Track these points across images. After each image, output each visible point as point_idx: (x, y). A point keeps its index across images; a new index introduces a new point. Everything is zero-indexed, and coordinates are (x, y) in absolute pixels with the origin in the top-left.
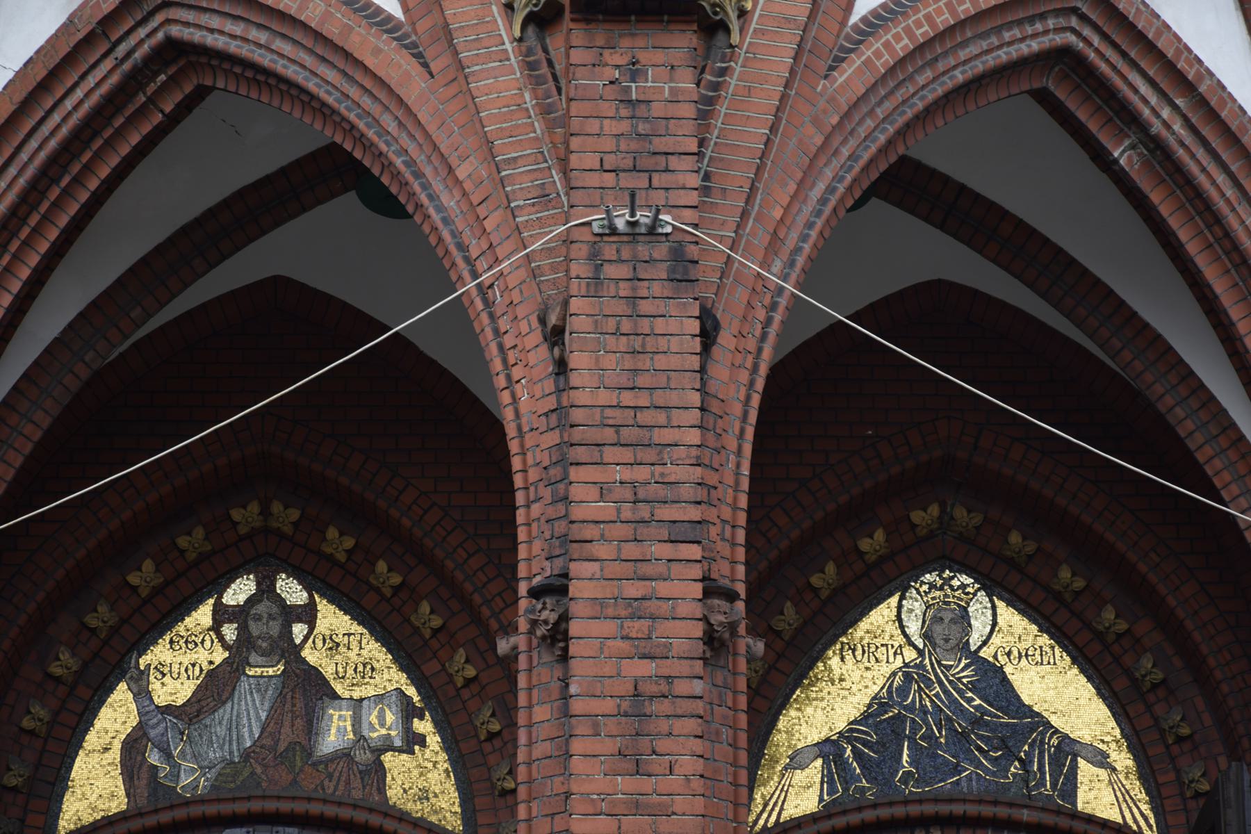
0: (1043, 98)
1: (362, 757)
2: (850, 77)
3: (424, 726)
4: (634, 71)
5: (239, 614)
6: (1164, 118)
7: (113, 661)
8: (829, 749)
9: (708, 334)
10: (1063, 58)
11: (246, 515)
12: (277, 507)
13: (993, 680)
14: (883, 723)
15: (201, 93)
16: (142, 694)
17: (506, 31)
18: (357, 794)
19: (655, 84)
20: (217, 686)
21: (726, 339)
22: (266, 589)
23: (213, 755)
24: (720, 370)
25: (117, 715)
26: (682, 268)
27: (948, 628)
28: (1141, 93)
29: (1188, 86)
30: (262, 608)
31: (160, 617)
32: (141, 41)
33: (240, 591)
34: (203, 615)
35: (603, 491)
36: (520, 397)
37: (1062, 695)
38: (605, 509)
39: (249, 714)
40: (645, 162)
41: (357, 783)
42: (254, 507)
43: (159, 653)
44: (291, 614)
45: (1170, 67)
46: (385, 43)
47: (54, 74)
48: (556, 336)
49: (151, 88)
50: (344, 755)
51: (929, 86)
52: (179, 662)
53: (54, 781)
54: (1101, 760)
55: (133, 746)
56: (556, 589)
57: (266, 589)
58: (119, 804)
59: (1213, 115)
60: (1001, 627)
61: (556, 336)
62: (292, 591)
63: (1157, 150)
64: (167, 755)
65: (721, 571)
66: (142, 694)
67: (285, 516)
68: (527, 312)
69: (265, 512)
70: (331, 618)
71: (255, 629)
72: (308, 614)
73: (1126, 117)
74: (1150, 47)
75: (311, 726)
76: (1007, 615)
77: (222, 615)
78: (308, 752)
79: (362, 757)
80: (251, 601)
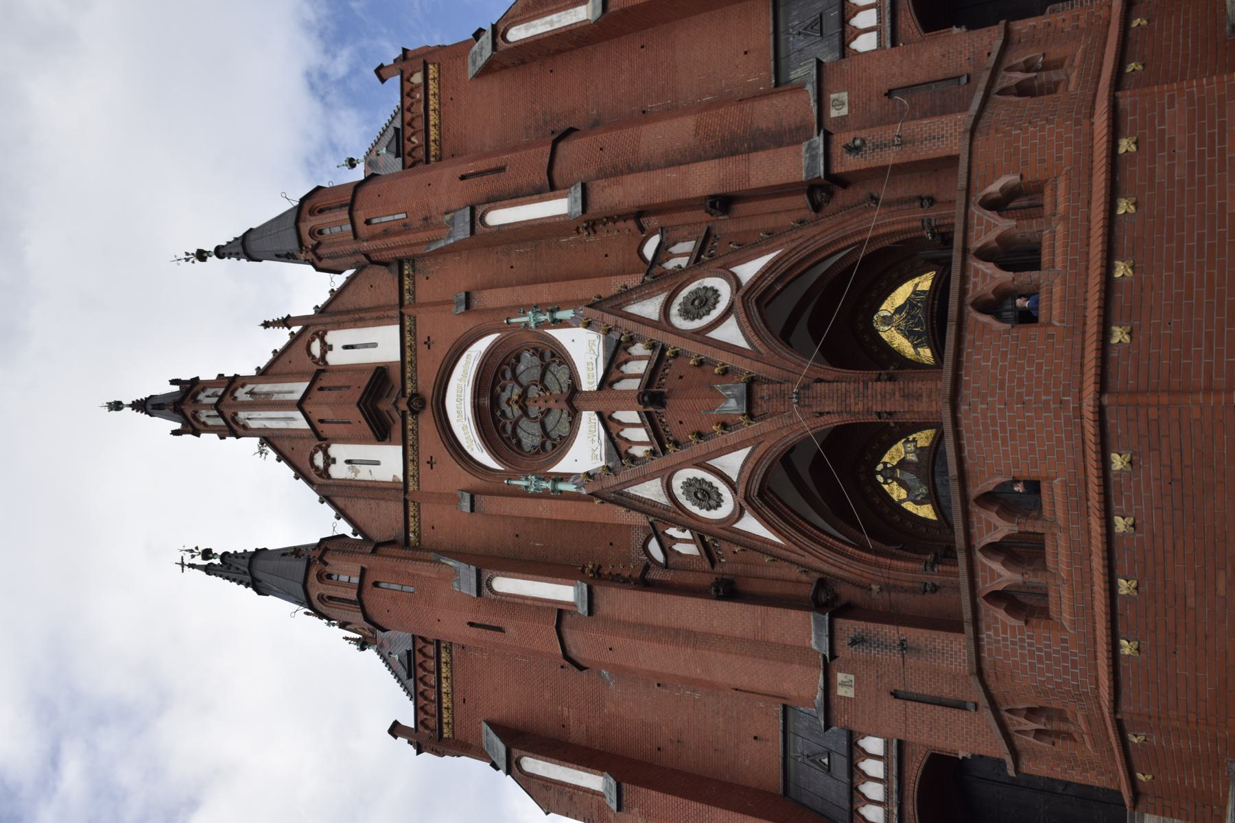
0: (766, 306)
2: (763, 349)
3: (911, 438)
4: (763, 398)
6: (770, 279)
7: (896, 507)
8: (915, 347)
9: (820, 381)
10: (757, 302)
13: (899, 310)
14: (908, 334)
15: (769, 489)
16: (904, 501)
17: (755, 425)
19: (764, 394)
20: (902, 484)
21: (821, 376)
22: (880, 473)
24: (829, 378)
25: (909, 506)
26: (805, 387)
27: (887, 321)
28: (765, 284)
29: (763, 274)
31: (886, 497)
32: (758, 502)
33: (880, 479)
34: (886, 487)
35: (856, 404)
36: (835, 420)
37: (901, 295)
38: (860, 405)
39: (909, 477)
40: (783, 396)
43: (895, 496)
45: (759, 278)
46: (758, 450)
47: (765, 520)
48: (821, 414)
50: (918, 456)
51: (765, 332)
52: (897, 492)
53: (925, 520)
54: (917, 285)
55: (916, 503)
56: (879, 414)
57: (880, 473)
58: (930, 506)
59: (770, 268)
60: (887, 308)
61: (821, 414)
62: (880, 467)
63: (778, 280)
65: (874, 377)
66: (904, 501)
68: (816, 420)
70: (886, 458)
72: (885, 464)
73: (770, 287)
74: (755, 283)
75: (911, 463)
76: (883, 307)
77: (886, 483)
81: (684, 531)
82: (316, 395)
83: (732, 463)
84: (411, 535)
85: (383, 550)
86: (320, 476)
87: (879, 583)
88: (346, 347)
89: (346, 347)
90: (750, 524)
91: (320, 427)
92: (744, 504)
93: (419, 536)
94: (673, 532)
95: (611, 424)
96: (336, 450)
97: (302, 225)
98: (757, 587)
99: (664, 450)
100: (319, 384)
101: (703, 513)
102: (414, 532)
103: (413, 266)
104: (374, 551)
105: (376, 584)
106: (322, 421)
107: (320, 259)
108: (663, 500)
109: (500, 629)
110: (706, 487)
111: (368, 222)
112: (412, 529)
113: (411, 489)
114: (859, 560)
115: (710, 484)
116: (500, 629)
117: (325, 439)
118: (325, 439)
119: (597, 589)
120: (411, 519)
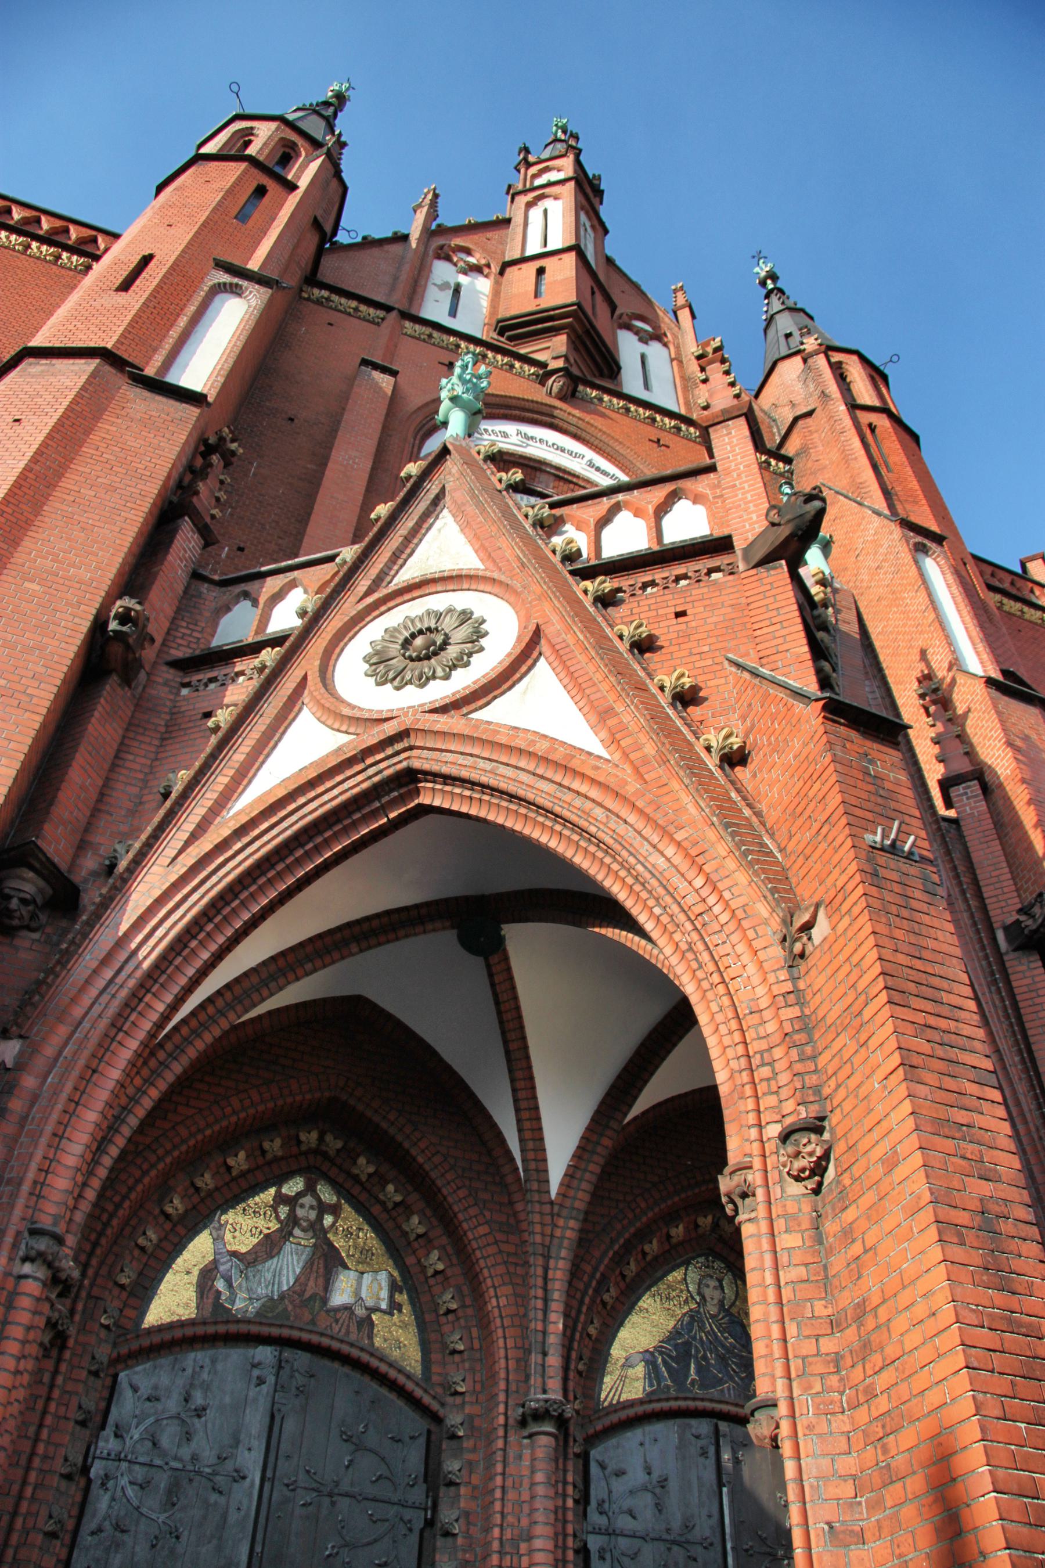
1: (360, 1312)
3: (402, 1298)
5: (292, 1202)
11: (310, 1138)
12: (329, 1138)
18: (353, 1337)
20: (270, 1246)
23: (261, 1291)
25: (200, 1249)
30: (308, 1200)
31: (236, 1192)
32: (388, 767)
33: (293, 1187)
39: (288, 1267)
41: (354, 1329)
42: (314, 1135)
44: (322, 1208)
49: (384, 800)
50: (347, 1308)
52: (244, 1226)
53: (145, 1289)
55: (207, 1275)
58: (189, 1312)
62: (327, 1195)
64: (230, 1286)
66: (218, 1239)
67: (332, 1143)
69: (321, 1139)
71: (300, 1212)
77: (280, 1199)
78: (325, 1301)
79: (360, 1312)
80: (300, 1195)
81: (302, 613)
82: (588, 282)
83: (545, 708)
84: (325, 293)
85: (311, 241)
86: (441, 247)
87: (21, 1065)
88: (643, 358)
89: (643, 358)
90: (307, 744)
91: (531, 268)
92: (390, 729)
93: (318, 302)
94: (297, 598)
95: (659, 493)
96: (483, 285)
97: (855, 358)
98: (101, 727)
99: (587, 573)
100: (599, 297)
101: (374, 631)
102: (328, 299)
103: (782, 475)
104: (316, 224)
105: (260, 191)
106: (541, 271)
107: (805, 361)
108: (409, 572)
109: (126, 286)
110: (452, 651)
111: (872, 428)
112: (335, 298)
113: (408, 324)
114: (118, 1025)
115: (462, 661)
116: (126, 286)
117: (502, 273)
118: (502, 273)
119: (192, 412)
120: (354, 304)
